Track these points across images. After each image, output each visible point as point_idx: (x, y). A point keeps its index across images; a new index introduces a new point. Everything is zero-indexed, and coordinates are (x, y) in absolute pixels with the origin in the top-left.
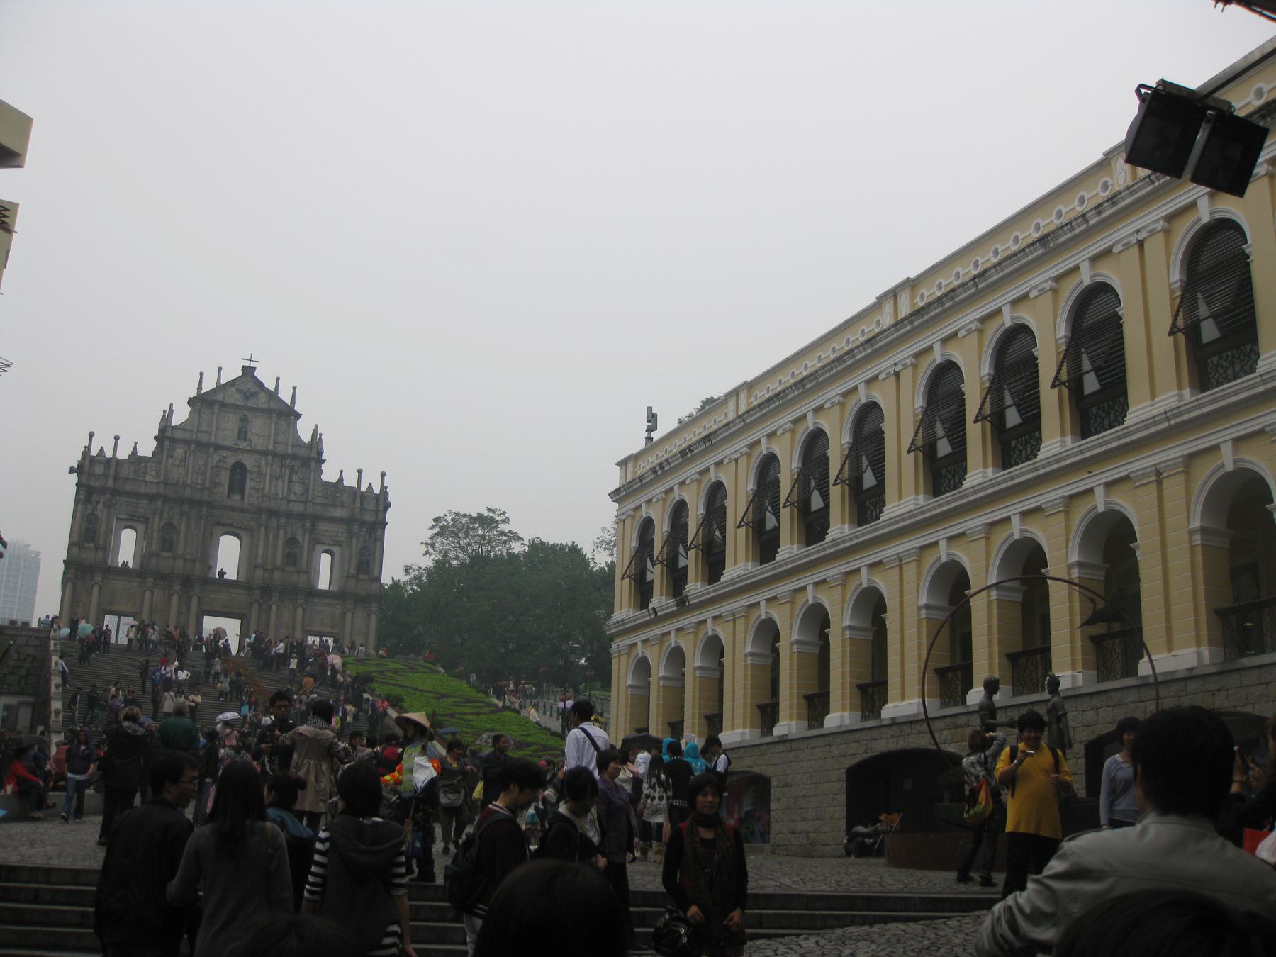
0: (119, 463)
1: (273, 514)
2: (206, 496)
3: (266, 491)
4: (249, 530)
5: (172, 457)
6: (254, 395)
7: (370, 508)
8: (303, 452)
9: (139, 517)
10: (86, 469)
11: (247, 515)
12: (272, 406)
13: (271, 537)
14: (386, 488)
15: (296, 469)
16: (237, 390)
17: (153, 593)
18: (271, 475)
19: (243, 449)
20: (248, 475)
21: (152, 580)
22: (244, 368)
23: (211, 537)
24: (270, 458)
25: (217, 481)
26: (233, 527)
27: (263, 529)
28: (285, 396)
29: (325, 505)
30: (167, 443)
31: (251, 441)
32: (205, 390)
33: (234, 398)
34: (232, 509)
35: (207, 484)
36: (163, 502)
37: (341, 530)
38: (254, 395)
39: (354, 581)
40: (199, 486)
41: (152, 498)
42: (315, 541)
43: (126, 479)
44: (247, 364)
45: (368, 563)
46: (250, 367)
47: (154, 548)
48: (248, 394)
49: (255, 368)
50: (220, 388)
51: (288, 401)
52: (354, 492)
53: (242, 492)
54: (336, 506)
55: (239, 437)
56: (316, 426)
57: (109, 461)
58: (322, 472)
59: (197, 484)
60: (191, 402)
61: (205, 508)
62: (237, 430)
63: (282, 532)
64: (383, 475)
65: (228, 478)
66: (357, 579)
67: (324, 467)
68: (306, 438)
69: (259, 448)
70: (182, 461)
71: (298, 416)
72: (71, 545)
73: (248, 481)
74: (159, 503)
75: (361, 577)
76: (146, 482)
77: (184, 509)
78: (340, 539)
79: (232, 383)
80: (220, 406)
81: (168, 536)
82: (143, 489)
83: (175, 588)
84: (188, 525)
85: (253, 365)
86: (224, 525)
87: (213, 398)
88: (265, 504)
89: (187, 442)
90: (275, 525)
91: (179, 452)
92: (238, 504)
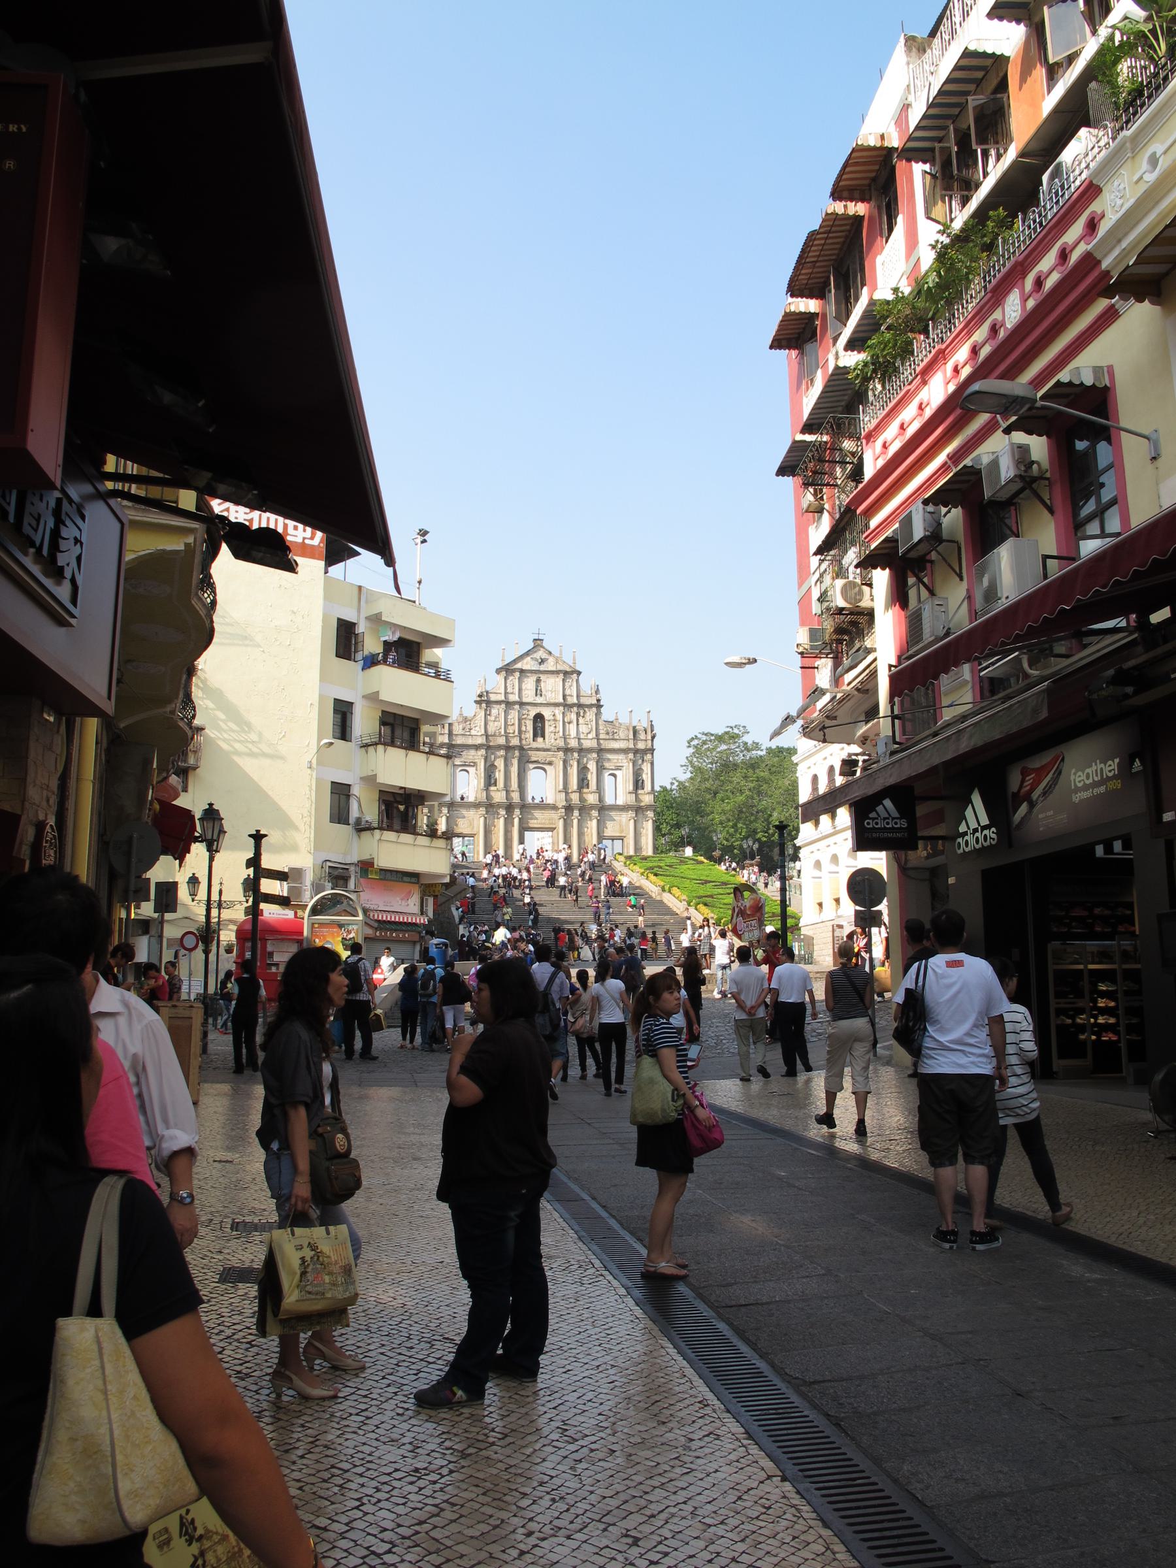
6: (542, 661)
12: (560, 668)
20: (546, 723)
34: (538, 749)
41: (477, 747)
53: (543, 736)
68: (586, 688)
69: (552, 701)
70: (496, 717)
71: (579, 673)
82: (470, 741)
91: (494, 711)
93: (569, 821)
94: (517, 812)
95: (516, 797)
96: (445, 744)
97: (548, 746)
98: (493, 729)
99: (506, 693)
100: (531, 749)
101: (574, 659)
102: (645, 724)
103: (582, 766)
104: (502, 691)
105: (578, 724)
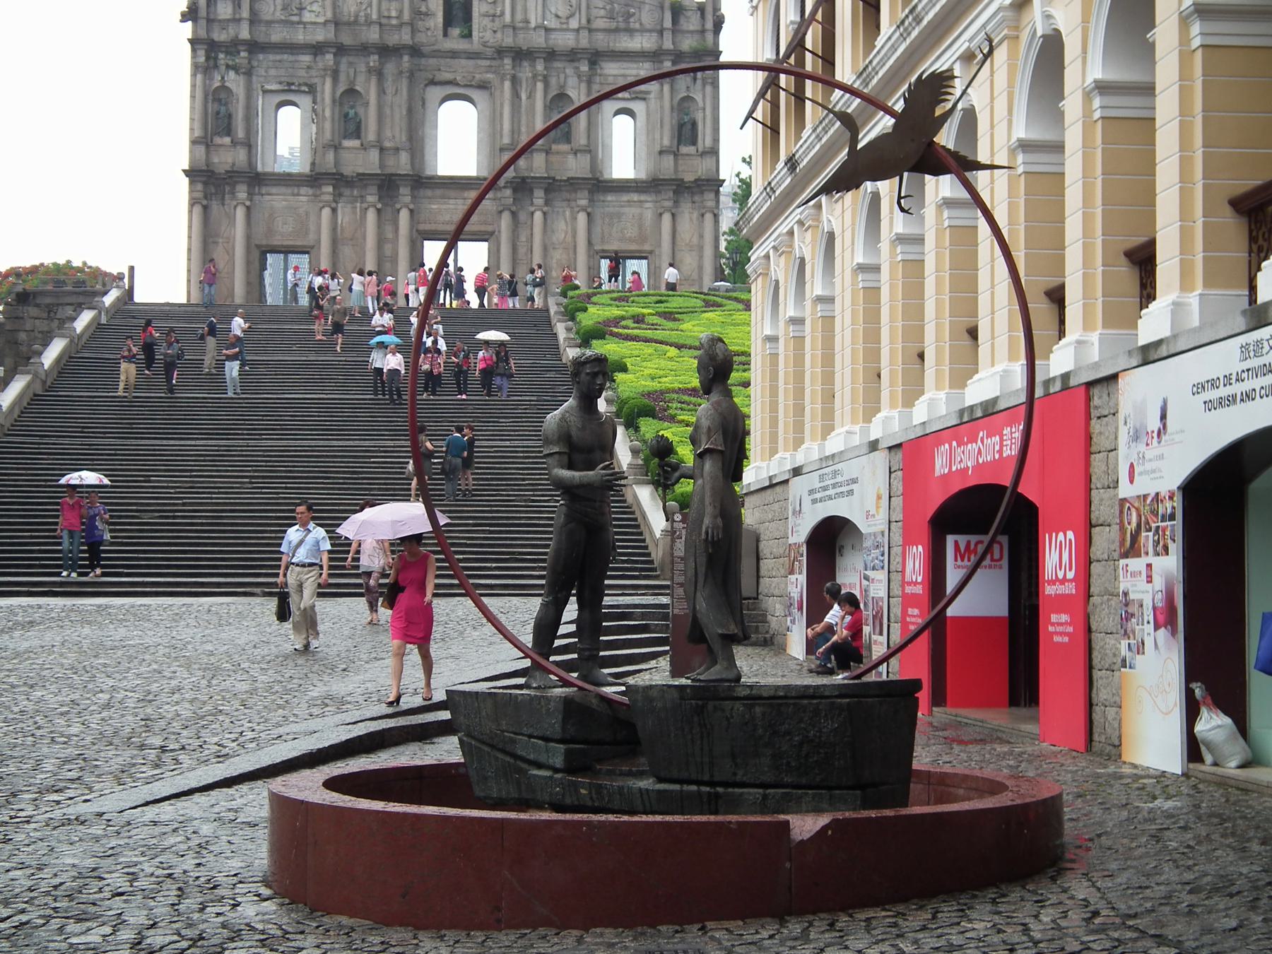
1: (521, 55)
2: (405, 37)
3: (508, 18)
4: (483, 86)
7: (691, 28)
9: (300, 85)
10: (203, 12)
11: (480, 62)
13: (524, 97)
17: (334, 210)
21: (330, 189)
23: (424, 104)
25: (423, 9)
26: (458, 85)
27: (507, 84)
29: (608, 31)
34: (454, 54)
35: (406, 16)
36: (335, 55)
39: (672, 157)
40: (394, 22)
41: (317, 49)
43: (269, 23)
45: (694, 124)
47: (328, 135)
59: (389, 17)
61: (406, 58)
63: (540, 86)
66: (676, 155)
72: (194, 142)
75: (685, 149)
76: (304, 24)
77: (372, 64)
81: (352, 112)
82: (300, 37)
83: (370, 199)
84: (382, 91)
88: (508, 41)
92: (462, 45)
93: (523, 216)
94: (405, 192)
96: (245, 42)
103: (553, 92)
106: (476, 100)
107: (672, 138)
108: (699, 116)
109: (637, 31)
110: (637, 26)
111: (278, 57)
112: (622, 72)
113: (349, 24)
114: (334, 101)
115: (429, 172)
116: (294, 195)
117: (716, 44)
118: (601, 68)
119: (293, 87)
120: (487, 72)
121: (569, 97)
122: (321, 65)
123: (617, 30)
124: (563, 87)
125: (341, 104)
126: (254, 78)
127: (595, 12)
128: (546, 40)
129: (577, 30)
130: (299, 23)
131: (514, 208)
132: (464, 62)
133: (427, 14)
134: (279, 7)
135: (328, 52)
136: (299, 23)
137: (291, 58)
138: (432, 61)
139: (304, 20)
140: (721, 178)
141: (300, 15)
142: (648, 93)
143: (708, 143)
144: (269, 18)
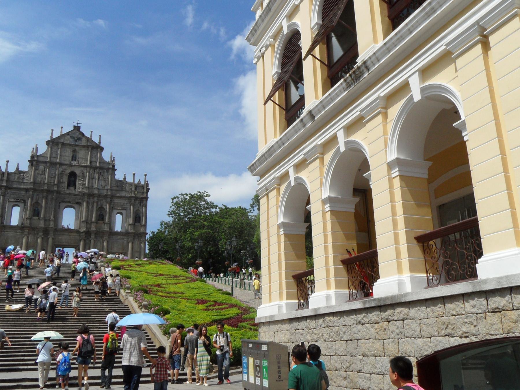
0: (9, 174)
2: (56, 189)
3: (87, 185)
4: (78, 203)
5: (37, 170)
8: (105, 166)
9: (21, 200)
11: (78, 197)
12: (89, 144)
13: (90, 207)
14: (147, 181)
15: (102, 174)
16: (71, 137)
17: (28, 237)
18: (89, 177)
19: (74, 165)
20: (77, 178)
21: (27, 231)
22: (75, 126)
23: (59, 208)
24: (88, 169)
25: (61, 181)
27: (85, 204)
28: (96, 139)
29: (117, 190)
30: (34, 163)
31: (78, 161)
32: (55, 136)
33: (68, 140)
34: (70, 194)
36: (33, 192)
37: (126, 202)
38: (79, 139)
40: (52, 184)
41: (27, 190)
42: (112, 209)
44: (76, 125)
45: (140, 218)
46: (77, 126)
48: (76, 139)
49: (80, 127)
50: (62, 136)
51: (97, 142)
52: (131, 184)
53: (75, 185)
54: (123, 191)
55: (72, 160)
56: (112, 153)
57: (3, 173)
58: (115, 175)
60: (48, 143)
61: (55, 194)
62: (71, 156)
63: (95, 204)
64: (146, 175)
65: (67, 179)
67: (116, 172)
70: (42, 172)
71: (102, 149)
73: (77, 180)
74: (31, 193)
75: (137, 224)
77: (44, 195)
78: (125, 206)
79: (68, 134)
80: (62, 145)
81: (37, 209)
84: (46, 203)
85: (79, 125)
86: (66, 202)
87: (58, 141)
89: (46, 162)
90: (92, 201)
91: (41, 167)
93: (87, 241)
94: (51, 233)
95: (52, 225)
97: (77, 193)
98: (39, 180)
99: (50, 157)
100: (65, 194)
101: (100, 140)
102: (143, 183)
103: (99, 206)
104: (49, 155)
105: (99, 180)
106: (75, 207)
107: (133, 220)
108: (141, 215)
109: (125, 191)
110: (125, 190)
111: (14, 192)
112: (120, 202)
113: (38, 183)
114: (31, 205)
115: (60, 227)
116: (15, 232)
117: (147, 196)
118: (114, 200)
119: (18, 201)
120: (80, 200)
121: (104, 208)
122: (28, 194)
123: (119, 190)
124: (102, 205)
125: (33, 206)
126: (6, 197)
127: (112, 185)
128: (98, 192)
129: (107, 190)
130: (22, 182)
131: (85, 239)
132: (73, 196)
133: (62, 182)
134: (16, 177)
135: (31, 191)
136: (22, 182)
137: (19, 192)
138: (62, 195)
139: (24, 181)
140: (147, 232)
141: (23, 180)
142: (127, 208)
143: (143, 223)
144: (13, 180)
